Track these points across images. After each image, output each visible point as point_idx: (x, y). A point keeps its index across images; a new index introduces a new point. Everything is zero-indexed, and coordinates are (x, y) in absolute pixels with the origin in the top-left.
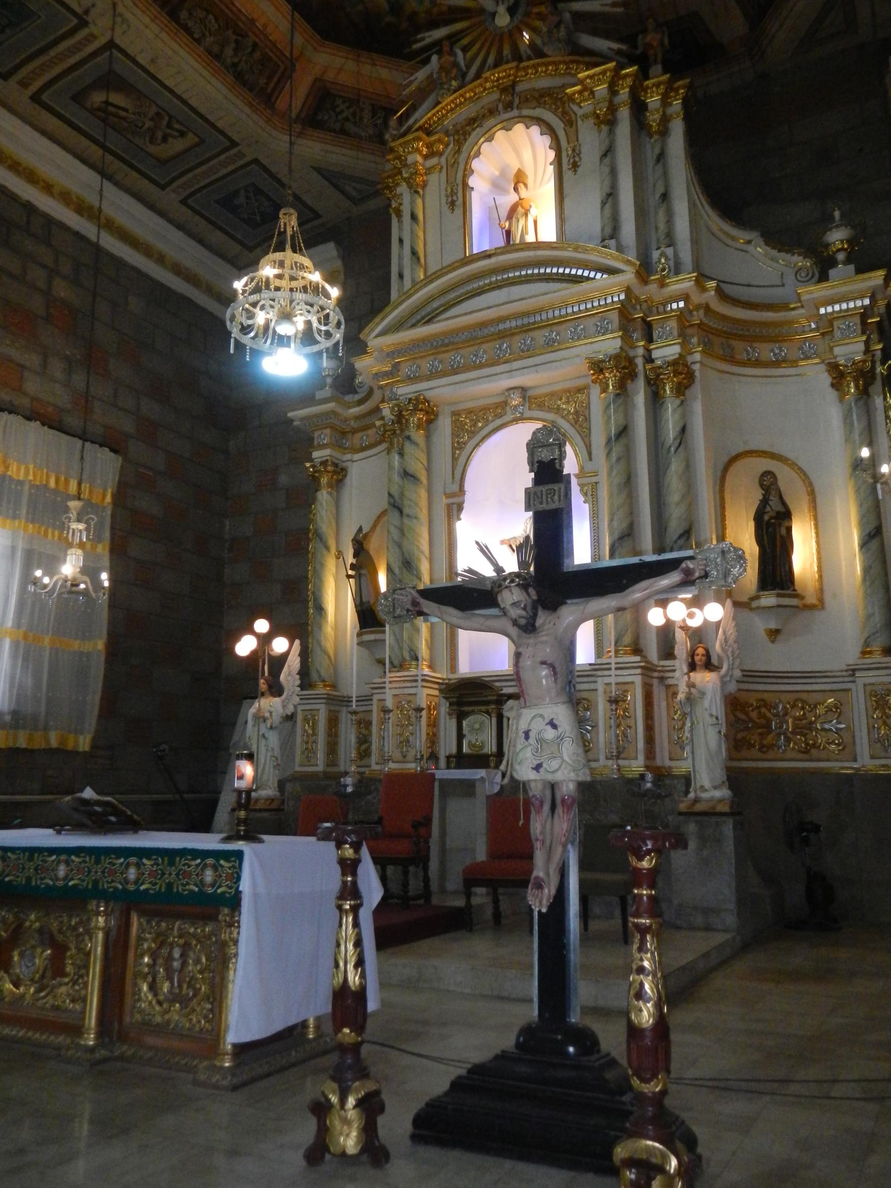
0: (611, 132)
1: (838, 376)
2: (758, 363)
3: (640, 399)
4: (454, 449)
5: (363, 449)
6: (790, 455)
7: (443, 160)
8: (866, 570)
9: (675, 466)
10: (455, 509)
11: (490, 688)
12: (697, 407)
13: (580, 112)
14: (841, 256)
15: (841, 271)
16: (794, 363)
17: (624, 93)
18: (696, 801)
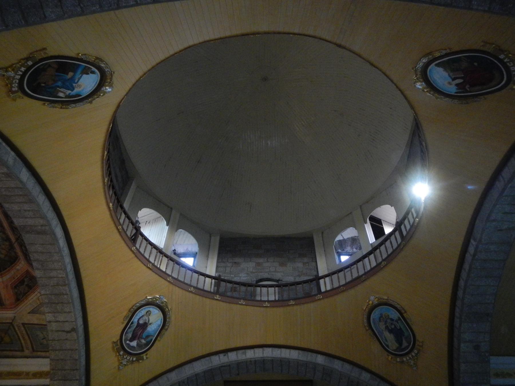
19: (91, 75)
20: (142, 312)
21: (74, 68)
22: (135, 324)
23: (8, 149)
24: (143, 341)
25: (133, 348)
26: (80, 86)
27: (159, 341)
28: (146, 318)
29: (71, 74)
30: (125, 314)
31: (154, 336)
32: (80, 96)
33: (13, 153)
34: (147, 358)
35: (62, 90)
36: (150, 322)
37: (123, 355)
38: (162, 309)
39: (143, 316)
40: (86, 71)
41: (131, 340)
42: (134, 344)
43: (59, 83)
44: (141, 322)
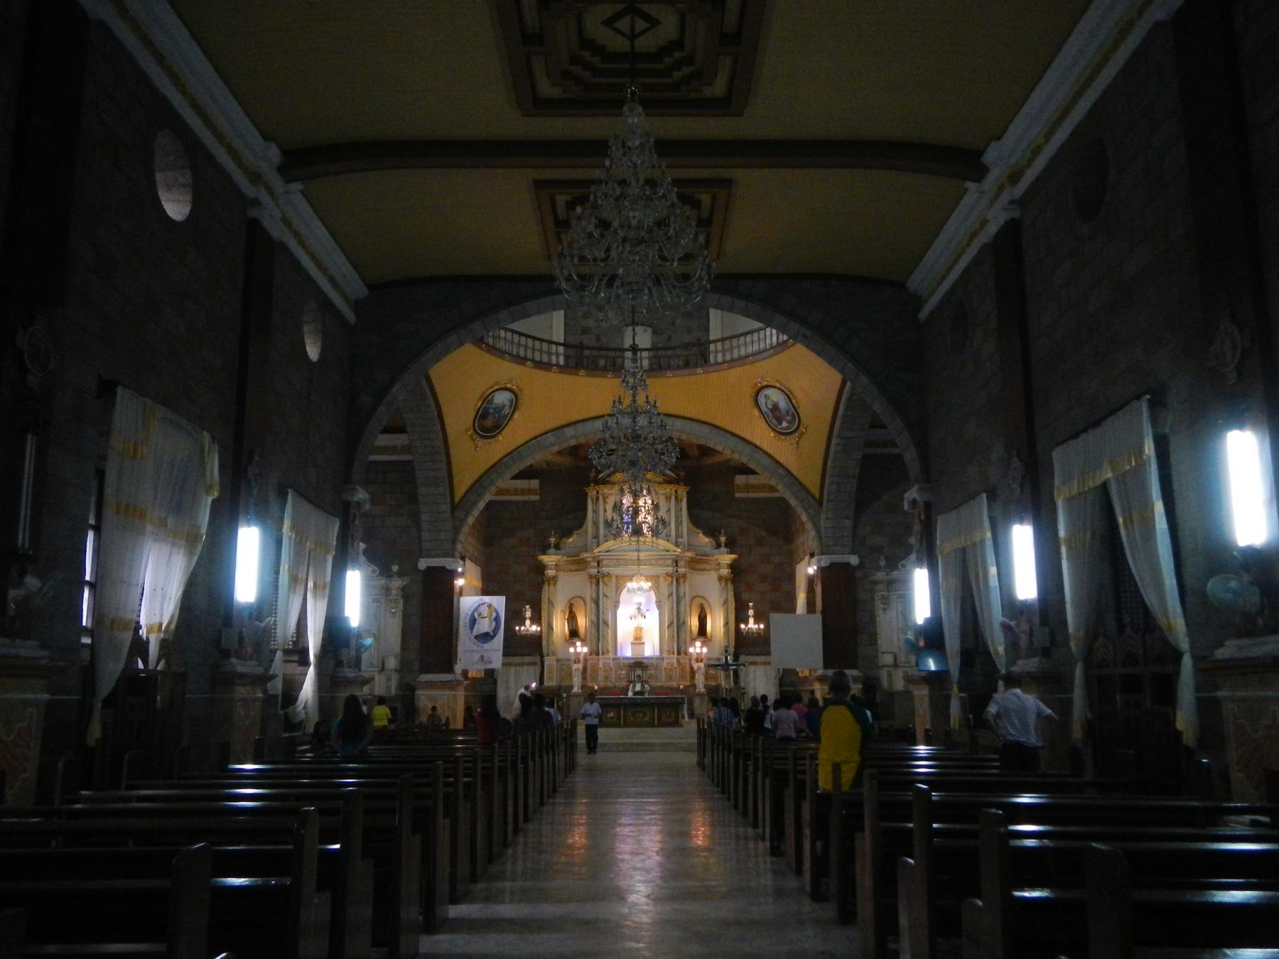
0: (670, 504)
1: (720, 578)
2: (698, 570)
3: (675, 583)
4: (616, 587)
5: (564, 571)
6: (705, 597)
7: (614, 492)
8: (725, 633)
9: (683, 603)
10: (616, 605)
11: (642, 663)
12: (687, 585)
13: (660, 492)
14: (723, 544)
15: (723, 549)
16: (708, 570)
17: (673, 491)
18: (699, 692)
19: (495, 398)
20: (762, 400)
23: (543, 437)
24: (788, 418)
25: (786, 428)
26: (503, 403)
27: (799, 407)
28: (769, 402)
29: (491, 410)
31: (791, 409)
32: (513, 400)
33: (550, 434)
34: (805, 429)
35: (503, 412)
36: (775, 401)
39: (766, 403)
40: (491, 402)
41: (780, 424)
42: (785, 424)
44: (770, 407)
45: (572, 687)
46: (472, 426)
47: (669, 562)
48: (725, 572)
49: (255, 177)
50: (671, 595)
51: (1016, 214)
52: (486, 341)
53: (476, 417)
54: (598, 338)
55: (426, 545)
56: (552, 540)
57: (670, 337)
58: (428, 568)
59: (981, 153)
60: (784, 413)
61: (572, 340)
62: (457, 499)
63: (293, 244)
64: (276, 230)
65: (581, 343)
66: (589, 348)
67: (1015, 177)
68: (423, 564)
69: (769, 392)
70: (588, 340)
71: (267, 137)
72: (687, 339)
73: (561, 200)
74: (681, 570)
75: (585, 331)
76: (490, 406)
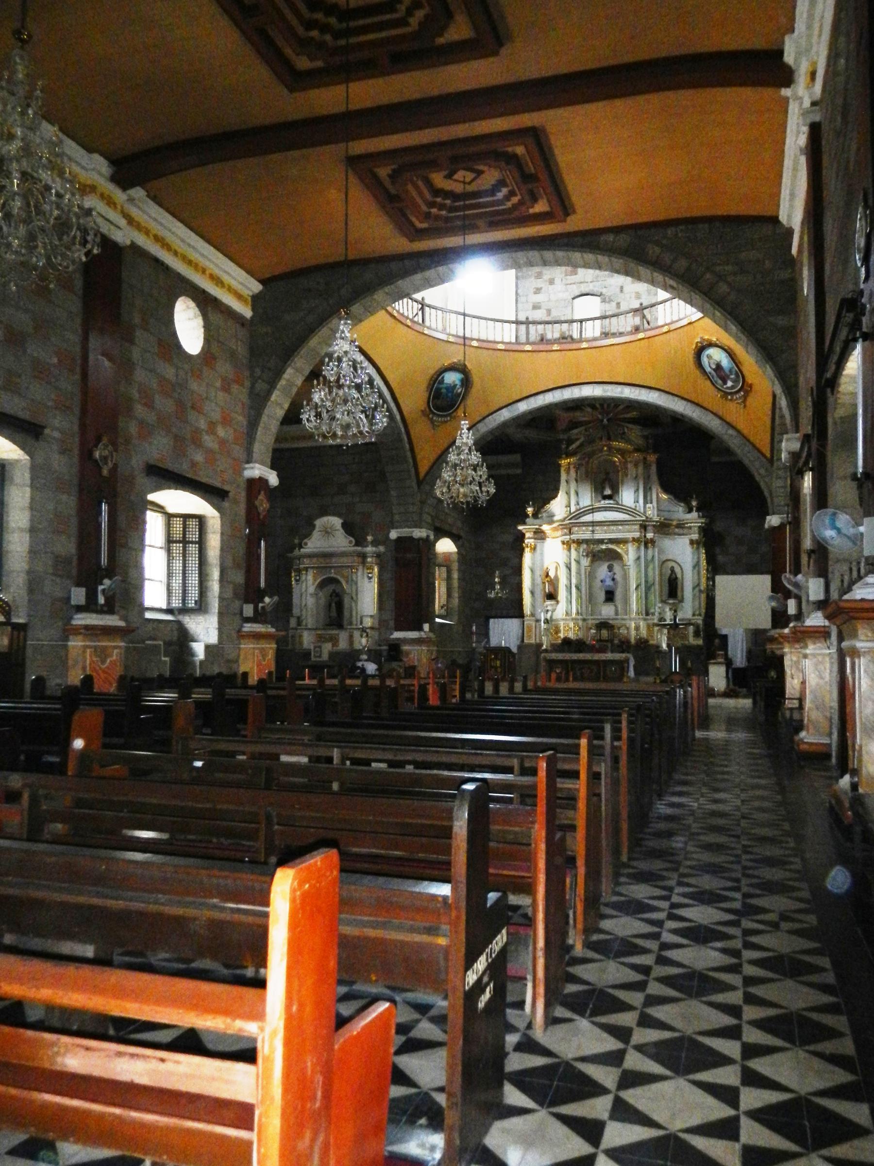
1: (692, 542)
3: (642, 548)
7: (584, 462)
9: (651, 567)
20: (705, 360)
21: (438, 390)
22: (713, 372)
24: (733, 376)
25: (732, 387)
28: (712, 361)
29: (444, 391)
30: (698, 372)
33: (504, 410)
37: (732, 397)
38: (711, 345)
40: (442, 381)
41: (725, 383)
42: (730, 384)
43: (450, 395)
44: (714, 367)
45: (542, 645)
46: (426, 405)
47: (637, 527)
48: (695, 536)
49: (87, 189)
50: (638, 558)
51: (817, 118)
52: (427, 323)
53: (429, 398)
54: (549, 312)
55: (397, 517)
56: (530, 510)
57: (618, 304)
58: (399, 539)
59: (781, 53)
60: (727, 371)
61: (522, 318)
62: (422, 475)
63: (155, 249)
64: (122, 236)
65: (527, 318)
66: (535, 323)
67: (813, 75)
68: (394, 535)
69: (711, 351)
70: (539, 315)
71: (90, 150)
72: (636, 305)
73: (383, 172)
74: (650, 535)
75: (536, 307)
76: (441, 386)
